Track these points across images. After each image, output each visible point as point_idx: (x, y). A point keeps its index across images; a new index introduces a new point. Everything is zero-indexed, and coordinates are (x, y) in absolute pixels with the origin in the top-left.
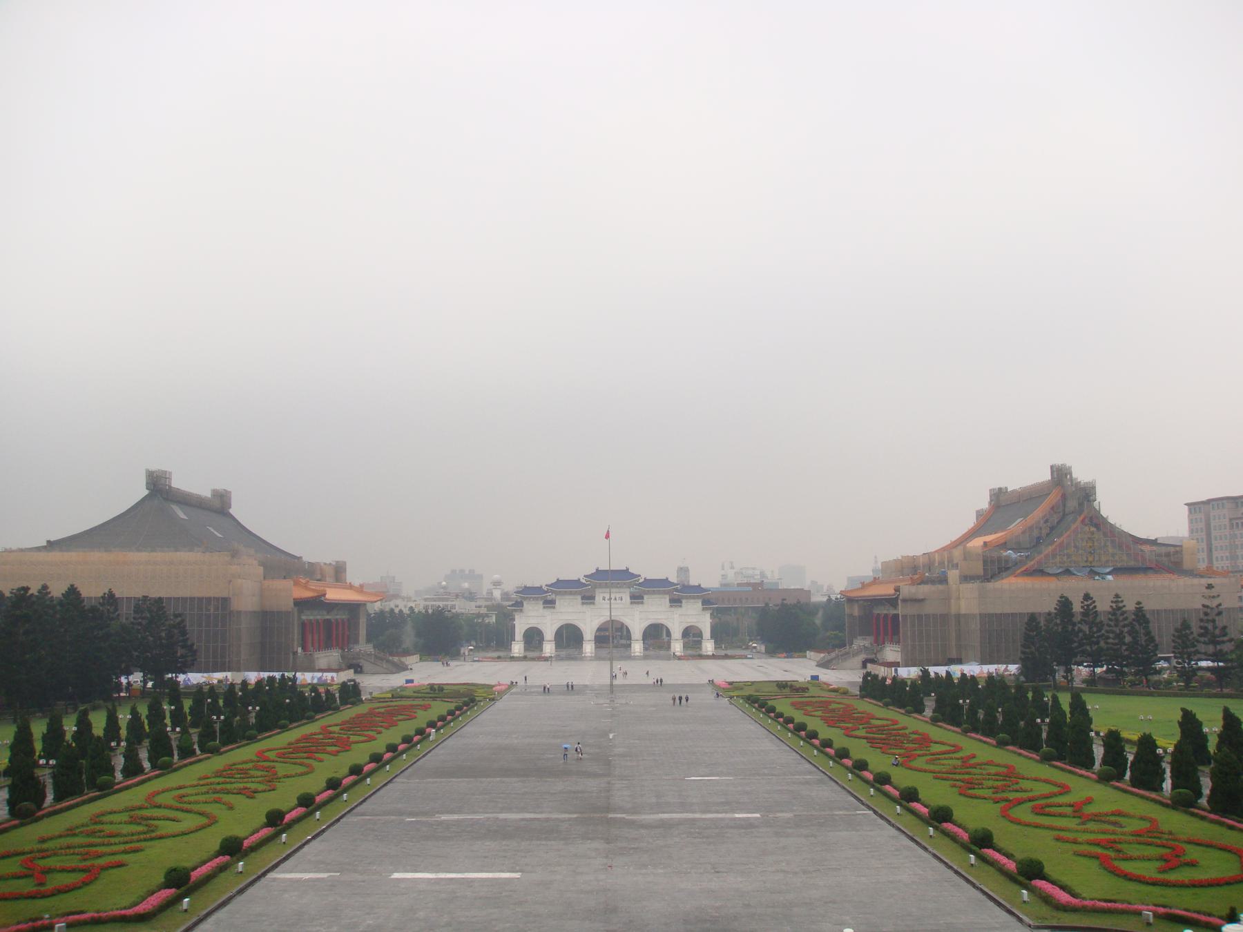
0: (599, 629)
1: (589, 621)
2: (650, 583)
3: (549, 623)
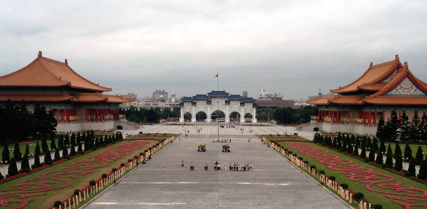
0: (213, 114)
1: (209, 111)
2: (232, 96)
3: (194, 111)
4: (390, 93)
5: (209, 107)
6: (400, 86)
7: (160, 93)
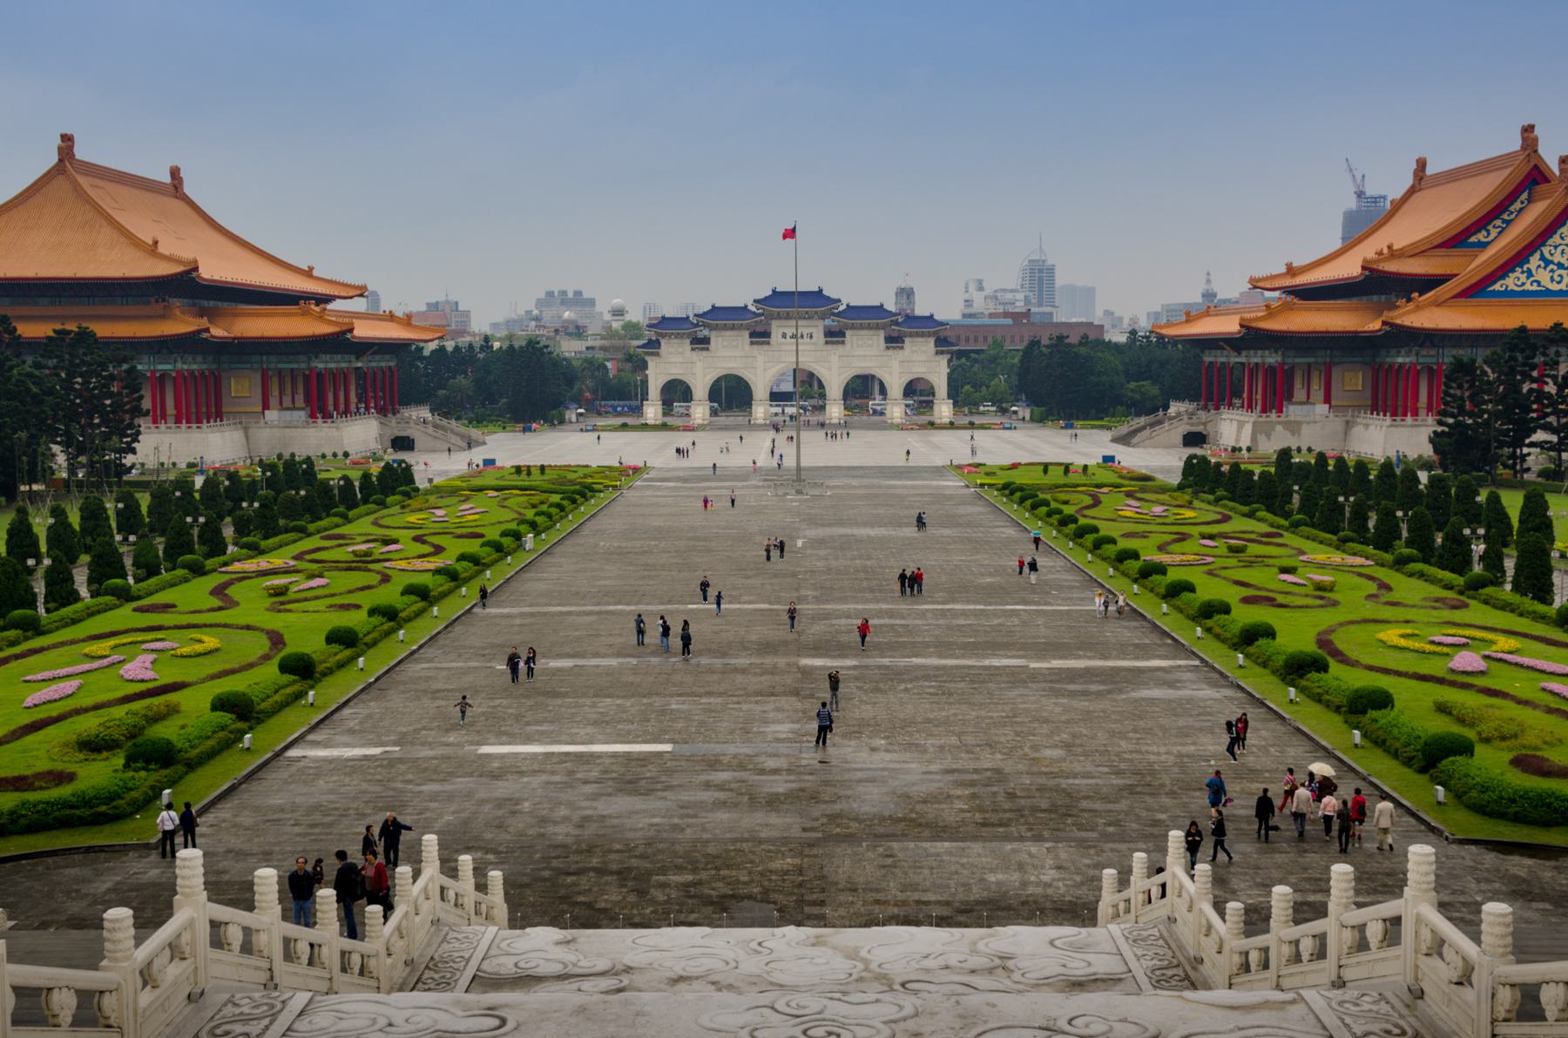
3: (701, 372)
4: (1497, 287)
5: (760, 354)
6: (1543, 258)
7: (564, 300)
